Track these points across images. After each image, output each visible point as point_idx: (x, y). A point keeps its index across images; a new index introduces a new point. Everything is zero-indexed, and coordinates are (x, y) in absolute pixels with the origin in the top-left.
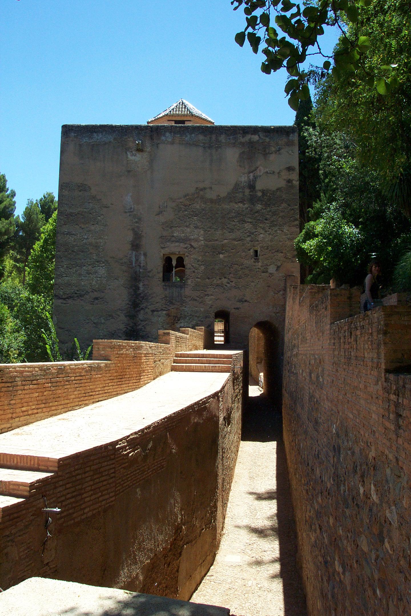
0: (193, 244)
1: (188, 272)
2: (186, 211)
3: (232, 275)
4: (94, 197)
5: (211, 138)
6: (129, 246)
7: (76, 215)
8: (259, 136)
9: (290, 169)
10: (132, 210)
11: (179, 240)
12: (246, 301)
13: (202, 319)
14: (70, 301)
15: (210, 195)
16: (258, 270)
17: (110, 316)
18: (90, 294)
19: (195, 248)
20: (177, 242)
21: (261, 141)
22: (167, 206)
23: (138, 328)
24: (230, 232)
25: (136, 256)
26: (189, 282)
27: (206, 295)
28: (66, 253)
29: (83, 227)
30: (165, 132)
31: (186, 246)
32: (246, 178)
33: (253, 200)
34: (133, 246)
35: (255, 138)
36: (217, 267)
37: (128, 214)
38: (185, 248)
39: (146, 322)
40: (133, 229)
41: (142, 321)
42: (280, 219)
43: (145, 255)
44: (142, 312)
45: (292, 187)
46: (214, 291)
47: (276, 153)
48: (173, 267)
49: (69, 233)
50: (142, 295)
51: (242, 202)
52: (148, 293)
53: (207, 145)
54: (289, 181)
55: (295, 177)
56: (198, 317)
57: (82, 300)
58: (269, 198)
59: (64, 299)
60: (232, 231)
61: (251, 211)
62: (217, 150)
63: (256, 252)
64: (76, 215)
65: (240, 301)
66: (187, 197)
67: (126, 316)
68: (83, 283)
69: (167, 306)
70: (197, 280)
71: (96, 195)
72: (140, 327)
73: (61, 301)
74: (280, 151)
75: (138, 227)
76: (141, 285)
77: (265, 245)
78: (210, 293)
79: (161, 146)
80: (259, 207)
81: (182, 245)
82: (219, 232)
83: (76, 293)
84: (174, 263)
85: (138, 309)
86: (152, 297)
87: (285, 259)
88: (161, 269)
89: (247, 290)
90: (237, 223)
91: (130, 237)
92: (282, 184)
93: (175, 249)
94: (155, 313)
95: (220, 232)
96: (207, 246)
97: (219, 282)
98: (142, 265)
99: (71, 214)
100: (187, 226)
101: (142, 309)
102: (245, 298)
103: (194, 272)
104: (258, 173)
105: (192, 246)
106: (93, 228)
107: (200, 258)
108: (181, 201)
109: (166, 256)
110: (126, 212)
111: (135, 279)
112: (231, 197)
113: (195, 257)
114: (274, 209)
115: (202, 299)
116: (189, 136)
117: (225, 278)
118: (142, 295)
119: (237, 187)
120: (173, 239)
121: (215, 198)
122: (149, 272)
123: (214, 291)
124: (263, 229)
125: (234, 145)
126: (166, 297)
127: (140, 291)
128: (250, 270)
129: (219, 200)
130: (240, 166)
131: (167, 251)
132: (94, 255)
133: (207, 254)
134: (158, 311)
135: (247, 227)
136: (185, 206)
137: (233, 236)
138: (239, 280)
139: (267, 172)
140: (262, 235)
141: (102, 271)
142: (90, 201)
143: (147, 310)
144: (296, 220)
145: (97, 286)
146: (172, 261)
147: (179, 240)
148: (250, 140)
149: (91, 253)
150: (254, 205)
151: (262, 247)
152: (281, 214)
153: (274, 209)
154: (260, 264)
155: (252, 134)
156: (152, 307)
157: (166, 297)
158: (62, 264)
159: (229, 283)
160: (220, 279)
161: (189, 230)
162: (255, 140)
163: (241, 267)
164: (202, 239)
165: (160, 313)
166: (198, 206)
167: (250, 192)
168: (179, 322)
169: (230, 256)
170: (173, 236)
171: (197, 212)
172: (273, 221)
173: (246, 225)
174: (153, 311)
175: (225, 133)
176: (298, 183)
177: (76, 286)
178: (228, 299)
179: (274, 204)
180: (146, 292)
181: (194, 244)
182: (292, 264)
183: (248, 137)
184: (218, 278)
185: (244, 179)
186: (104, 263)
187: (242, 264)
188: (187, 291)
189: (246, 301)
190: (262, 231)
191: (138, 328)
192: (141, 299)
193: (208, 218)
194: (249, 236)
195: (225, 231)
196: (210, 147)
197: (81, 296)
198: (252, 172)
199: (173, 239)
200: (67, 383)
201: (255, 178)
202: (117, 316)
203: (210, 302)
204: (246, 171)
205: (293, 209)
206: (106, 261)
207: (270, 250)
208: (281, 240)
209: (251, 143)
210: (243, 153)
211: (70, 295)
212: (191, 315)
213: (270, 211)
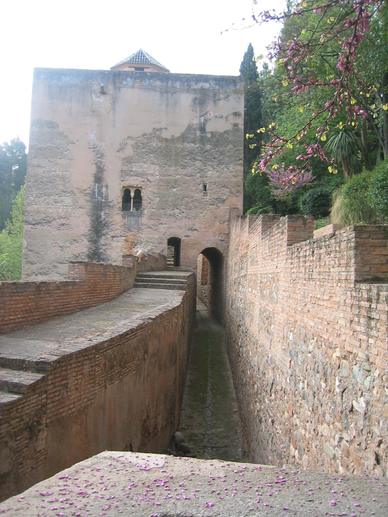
0: (149, 178)
2: (144, 148)
3: (183, 207)
4: (61, 134)
5: (167, 84)
6: (93, 179)
7: (45, 149)
8: (210, 84)
9: (236, 114)
10: (96, 146)
11: (137, 175)
12: (195, 230)
13: (157, 245)
14: (38, 227)
15: (166, 135)
16: (206, 202)
17: (75, 240)
18: (57, 220)
19: (151, 182)
20: (135, 176)
21: (211, 89)
22: (127, 144)
23: (99, 251)
24: (182, 169)
25: (98, 187)
26: (145, 212)
27: (160, 224)
28: (36, 184)
29: (51, 160)
30: (127, 77)
31: (143, 180)
32: (198, 121)
33: (203, 140)
35: (207, 86)
36: (170, 199)
37: (92, 150)
38: (143, 182)
39: (107, 247)
40: (96, 164)
41: (103, 245)
42: (227, 158)
43: (107, 187)
44: (103, 237)
45: (238, 130)
46: (167, 220)
47: (224, 100)
48: (131, 198)
49: (39, 166)
50: (103, 222)
51: (193, 142)
52: (109, 220)
53: (163, 90)
54: (236, 125)
55: (241, 121)
56: (153, 243)
57: (49, 226)
58: (218, 139)
59: (34, 224)
60: (184, 167)
61: (202, 150)
62: (172, 96)
63: (205, 186)
64: (45, 149)
65: (191, 229)
66: (145, 136)
67: (89, 241)
68: (50, 211)
69: (125, 233)
70: (152, 210)
71: (63, 132)
72: (101, 251)
73: (31, 226)
74: (229, 98)
75: (101, 162)
76: (102, 213)
77: (213, 181)
78: (163, 222)
79: (123, 90)
80: (208, 147)
81: (139, 178)
82: (173, 168)
83: (44, 220)
84: (132, 194)
85: (100, 235)
86: (112, 225)
87: (230, 194)
88: (120, 200)
89: (197, 220)
90: (189, 161)
91: (93, 170)
92: (229, 127)
93: (134, 181)
94: (115, 239)
95: (173, 168)
96: (162, 180)
97: (172, 212)
98: (104, 196)
100: (144, 162)
101: (103, 234)
102: (195, 227)
103: (150, 203)
104: (208, 116)
105: (148, 180)
106: (60, 161)
107: (156, 191)
108: (140, 139)
109: (125, 189)
110: (90, 148)
112: (183, 138)
113: (151, 189)
114: (221, 149)
115: (157, 227)
116: (148, 82)
117: (178, 209)
118: (103, 222)
119: (190, 128)
120: (132, 173)
121: (169, 137)
122: (110, 202)
123: (167, 220)
124: (212, 166)
125: (188, 91)
126: (125, 224)
127: (102, 219)
128: (200, 203)
129: (173, 140)
130: (193, 110)
131: (126, 184)
132: (61, 186)
133: (162, 187)
134: (117, 237)
135: (197, 165)
136: (143, 144)
137: (185, 172)
138: (189, 211)
139: (216, 117)
140: (210, 172)
141: (68, 200)
142: (58, 137)
143: (107, 236)
144: (241, 159)
145: (63, 214)
146: (130, 193)
147: (137, 175)
148: (202, 87)
149: (58, 184)
150: (204, 146)
151: (210, 182)
152: (228, 154)
153: (221, 149)
154: (208, 197)
155: (204, 82)
156: (112, 234)
157: (125, 224)
158: (31, 193)
159: (180, 214)
160: (173, 210)
161: (146, 165)
162: (206, 88)
163: (191, 200)
164: (158, 174)
165: (119, 238)
166: (154, 144)
167: (201, 133)
168: (136, 247)
169: (181, 190)
170: (132, 171)
171: (154, 150)
172: (221, 160)
173: (197, 163)
174: (113, 237)
175: (180, 81)
176: (243, 127)
177: (44, 214)
178: (180, 228)
179: (222, 145)
180: (107, 220)
181: (150, 178)
182: (236, 198)
183: (200, 85)
184: (171, 208)
185: (196, 122)
186: (69, 193)
187: (192, 197)
188: (144, 220)
189: (195, 230)
190: (210, 168)
191: (99, 251)
192: (102, 226)
193: (163, 156)
194: (199, 172)
195: (178, 167)
196: (167, 92)
197: (49, 222)
198: (203, 116)
199: (132, 173)
200: (47, 295)
201: (206, 121)
202: (81, 241)
203: (163, 230)
204: (198, 115)
205: (238, 150)
206: (71, 191)
207: (217, 186)
208: (227, 177)
209: (202, 90)
211: (39, 221)
212: (146, 241)
213: (218, 151)
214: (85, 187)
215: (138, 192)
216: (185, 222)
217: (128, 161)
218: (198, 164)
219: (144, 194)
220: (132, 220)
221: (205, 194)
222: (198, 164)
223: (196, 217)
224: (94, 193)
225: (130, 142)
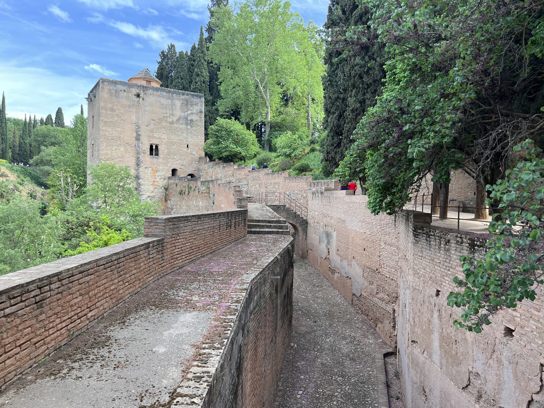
1: (160, 152)
14: (108, 162)
33: (187, 124)
34: (136, 138)
43: (142, 143)
65: (182, 165)
80: (189, 127)
84: (154, 148)
88: (149, 150)
93: (155, 142)
99: (107, 122)
111: (138, 153)
119: (180, 118)
131: (151, 142)
156: (145, 166)
181: (163, 141)
188: (160, 160)
210: (183, 103)
214: (131, 143)
215: (157, 147)
216: (179, 161)
217: (152, 131)
218: (185, 135)
219: (159, 147)
220: (155, 160)
221: (188, 149)
222: (185, 135)
223: (184, 159)
224: (136, 146)
225: (152, 121)
